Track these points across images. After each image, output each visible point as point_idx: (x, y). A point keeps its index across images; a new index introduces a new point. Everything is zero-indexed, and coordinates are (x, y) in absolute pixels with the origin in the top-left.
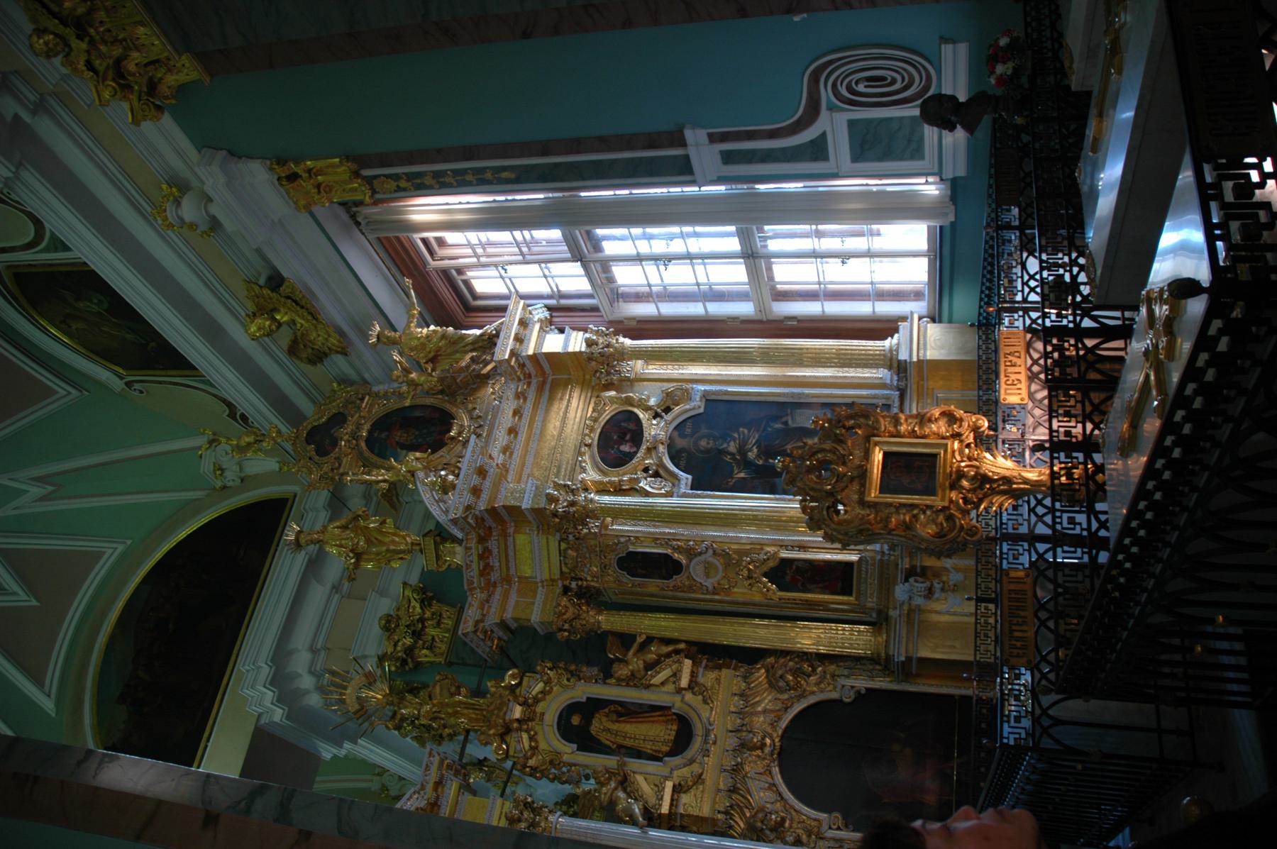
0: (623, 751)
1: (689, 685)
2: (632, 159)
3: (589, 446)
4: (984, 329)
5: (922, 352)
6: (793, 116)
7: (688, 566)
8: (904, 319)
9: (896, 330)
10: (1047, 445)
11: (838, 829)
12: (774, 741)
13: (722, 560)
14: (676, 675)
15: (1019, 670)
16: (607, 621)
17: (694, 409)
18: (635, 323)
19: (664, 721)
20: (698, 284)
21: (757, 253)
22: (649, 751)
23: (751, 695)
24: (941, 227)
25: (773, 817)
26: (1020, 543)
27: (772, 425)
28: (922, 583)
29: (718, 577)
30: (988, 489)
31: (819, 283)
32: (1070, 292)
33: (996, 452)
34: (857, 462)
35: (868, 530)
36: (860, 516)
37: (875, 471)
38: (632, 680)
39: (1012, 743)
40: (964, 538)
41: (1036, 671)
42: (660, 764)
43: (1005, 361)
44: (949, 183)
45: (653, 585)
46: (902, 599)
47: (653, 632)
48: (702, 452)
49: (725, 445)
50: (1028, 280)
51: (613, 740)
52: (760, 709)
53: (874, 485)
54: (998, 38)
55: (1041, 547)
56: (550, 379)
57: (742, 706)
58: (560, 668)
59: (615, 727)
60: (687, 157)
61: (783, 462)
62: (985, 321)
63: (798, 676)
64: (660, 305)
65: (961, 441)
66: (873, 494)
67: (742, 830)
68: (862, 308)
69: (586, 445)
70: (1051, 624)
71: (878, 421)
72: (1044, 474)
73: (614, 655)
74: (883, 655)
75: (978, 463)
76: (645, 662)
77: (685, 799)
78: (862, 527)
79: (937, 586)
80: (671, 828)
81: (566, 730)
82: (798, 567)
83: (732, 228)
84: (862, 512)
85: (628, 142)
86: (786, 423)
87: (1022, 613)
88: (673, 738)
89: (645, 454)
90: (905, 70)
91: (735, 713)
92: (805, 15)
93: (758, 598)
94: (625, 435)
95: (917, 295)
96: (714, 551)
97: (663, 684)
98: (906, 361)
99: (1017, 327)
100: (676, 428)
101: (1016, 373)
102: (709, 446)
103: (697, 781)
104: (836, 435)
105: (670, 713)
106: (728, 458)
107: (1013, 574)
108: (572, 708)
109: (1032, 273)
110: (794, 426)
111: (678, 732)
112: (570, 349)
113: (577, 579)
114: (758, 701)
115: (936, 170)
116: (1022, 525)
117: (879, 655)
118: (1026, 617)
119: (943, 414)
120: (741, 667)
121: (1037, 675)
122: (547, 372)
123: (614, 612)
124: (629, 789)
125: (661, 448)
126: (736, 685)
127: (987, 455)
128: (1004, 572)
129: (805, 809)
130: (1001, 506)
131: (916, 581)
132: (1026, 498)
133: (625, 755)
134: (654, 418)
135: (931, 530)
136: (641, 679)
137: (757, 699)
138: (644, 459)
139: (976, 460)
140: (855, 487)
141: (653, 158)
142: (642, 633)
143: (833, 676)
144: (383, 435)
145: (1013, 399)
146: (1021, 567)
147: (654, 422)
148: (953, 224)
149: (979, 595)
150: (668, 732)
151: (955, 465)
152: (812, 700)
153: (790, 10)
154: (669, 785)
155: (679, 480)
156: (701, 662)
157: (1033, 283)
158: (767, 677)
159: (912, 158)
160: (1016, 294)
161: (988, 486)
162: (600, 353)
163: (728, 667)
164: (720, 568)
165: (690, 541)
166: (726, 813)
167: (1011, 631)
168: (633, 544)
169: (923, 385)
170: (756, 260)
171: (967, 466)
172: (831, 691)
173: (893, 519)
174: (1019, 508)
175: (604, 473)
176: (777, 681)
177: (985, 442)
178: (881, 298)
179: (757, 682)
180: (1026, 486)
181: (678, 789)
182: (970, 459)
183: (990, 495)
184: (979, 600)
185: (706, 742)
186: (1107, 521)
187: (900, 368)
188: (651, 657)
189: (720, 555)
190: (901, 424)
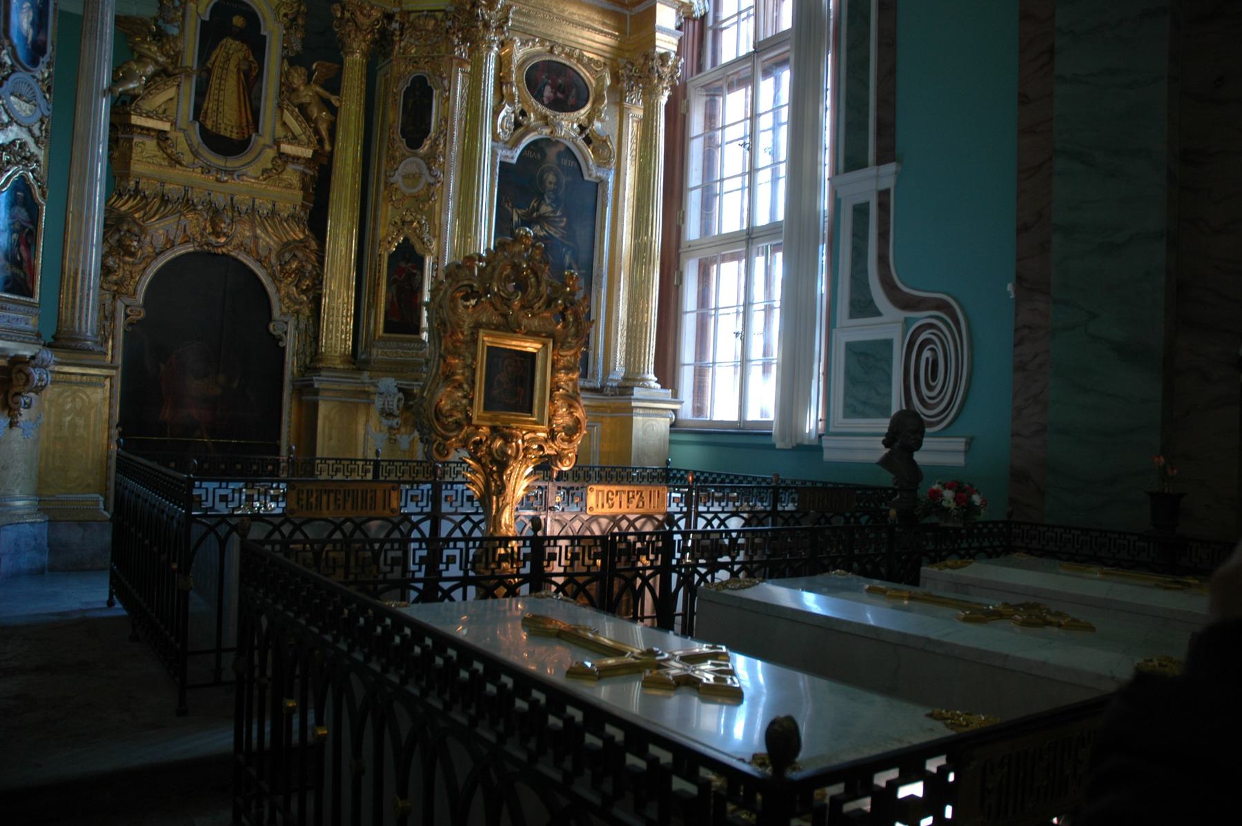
0: (204, 75)
1: (283, 154)
2: (867, 105)
3: (551, 51)
4: (664, 474)
5: (641, 411)
6: (903, 283)
7: (416, 155)
8: (675, 395)
9: (663, 387)
10: (540, 533)
11: (127, 316)
12: (223, 246)
13: (422, 192)
14: (294, 140)
15: (283, 501)
16: (355, 59)
17: (588, 169)
18: (682, 112)
19: (241, 123)
20: (722, 180)
21: (752, 244)
22: (205, 105)
23: (274, 223)
24: (770, 434)
25: (135, 243)
26: (430, 503)
27: (569, 252)
28: (398, 407)
29: (404, 189)
30: (491, 469)
31: (716, 309)
32: (711, 561)
33: (534, 478)
34: (525, 322)
35: (445, 332)
36: (461, 323)
37: (514, 343)
38: (286, 89)
39: (196, 492)
40: (435, 441)
41: (282, 519)
42: (191, 118)
43: (633, 492)
44: (816, 443)
45: (395, 117)
46: (380, 384)
47: (342, 113)
48: (541, 177)
50: (719, 519)
51: (216, 64)
52: (259, 231)
53: (498, 341)
54: (979, 494)
55: (426, 527)
56: (627, 12)
57: (261, 212)
58: (299, 6)
59: (232, 66)
60: (864, 165)
61: (526, 236)
62: (671, 475)
63: (296, 274)
64: (701, 140)
65: (546, 440)
66: (487, 339)
67: (118, 209)
68: (687, 353)
69: (552, 48)
70: (338, 535)
71: (571, 348)
72: (508, 530)
73: (315, 70)
74: (321, 365)
75: (521, 458)
76: (309, 104)
77: (151, 144)
78: (449, 325)
79: (394, 422)
80: (113, 126)
82: (415, 274)
83: (780, 216)
84: (466, 327)
85: (887, 101)
87: (349, 505)
88: (222, 133)
89: (541, 113)
90: (942, 400)
91: (253, 205)
92: (1012, 296)
93: (382, 232)
94: (563, 92)
95: (698, 410)
96: (433, 185)
97: (284, 124)
98: (632, 394)
99: (670, 506)
100: (568, 149)
101: (621, 502)
102: (548, 185)
103: (172, 159)
104: (557, 299)
105: (251, 131)
106: (534, 204)
107: (394, 495)
111: (230, 140)
112: (658, 35)
113: (402, 29)
114: (267, 231)
115: (832, 430)
116: (451, 506)
117: (321, 360)
118: (344, 508)
119: (578, 421)
120: (306, 213)
121: (277, 521)
122: (633, 9)
123: (364, 72)
124: (158, 79)
125: (546, 131)
126: (285, 206)
127: (530, 469)
128: (396, 485)
129: (146, 280)
130: (473, 483)
131: (399, 400)
132: (481, 511)
133: (199, 76)
134: (580, 126)
135: (445, 405)
136: (289, 99)
137: (269, 229)
138: (535, 112)
139: (525, 456)
140: (496, 319)
141: (866, 129)
142: (341, 102)
143: (297, 312)
145: (592, 499)
146: (403, 504)
147: (575, 126)
148: (772, 447)
149: (382, 463)
150: (229, 129)
151: (518, 433)
152: (271, 289)
153: (1019, 280)
154: (166, 126)
155: (511, 149)
156: (309, 168)
157: (716, 523)
158: (295, 240)
159: (846, 406)
160: (705, 505)
161: (494, 469)
162: (653, 68)
163: (304, 198)
164: (414, 191)
165: (444, 158)
166: (137, 191)
167: (328, 492)
168: (441, 94)
169: (606, 412)
170: (744, 242)
171: (518, 446)
172: (281, 309)
173: (457, 361)
174: (470, 503)
175: (520, 66)
176: (290, 251)
177: (544, 467)
178: (697, 373)
179: (288, 229)
180: (494, 511)
181: (161, 136)
182: (526, 449)
183: (484, 471)
184: (377, 464)
185: (219, 170)
186: (452, 599)
187: (625, 389)
188: (314, 112)
189: (428, 190)
190: (567, 374)
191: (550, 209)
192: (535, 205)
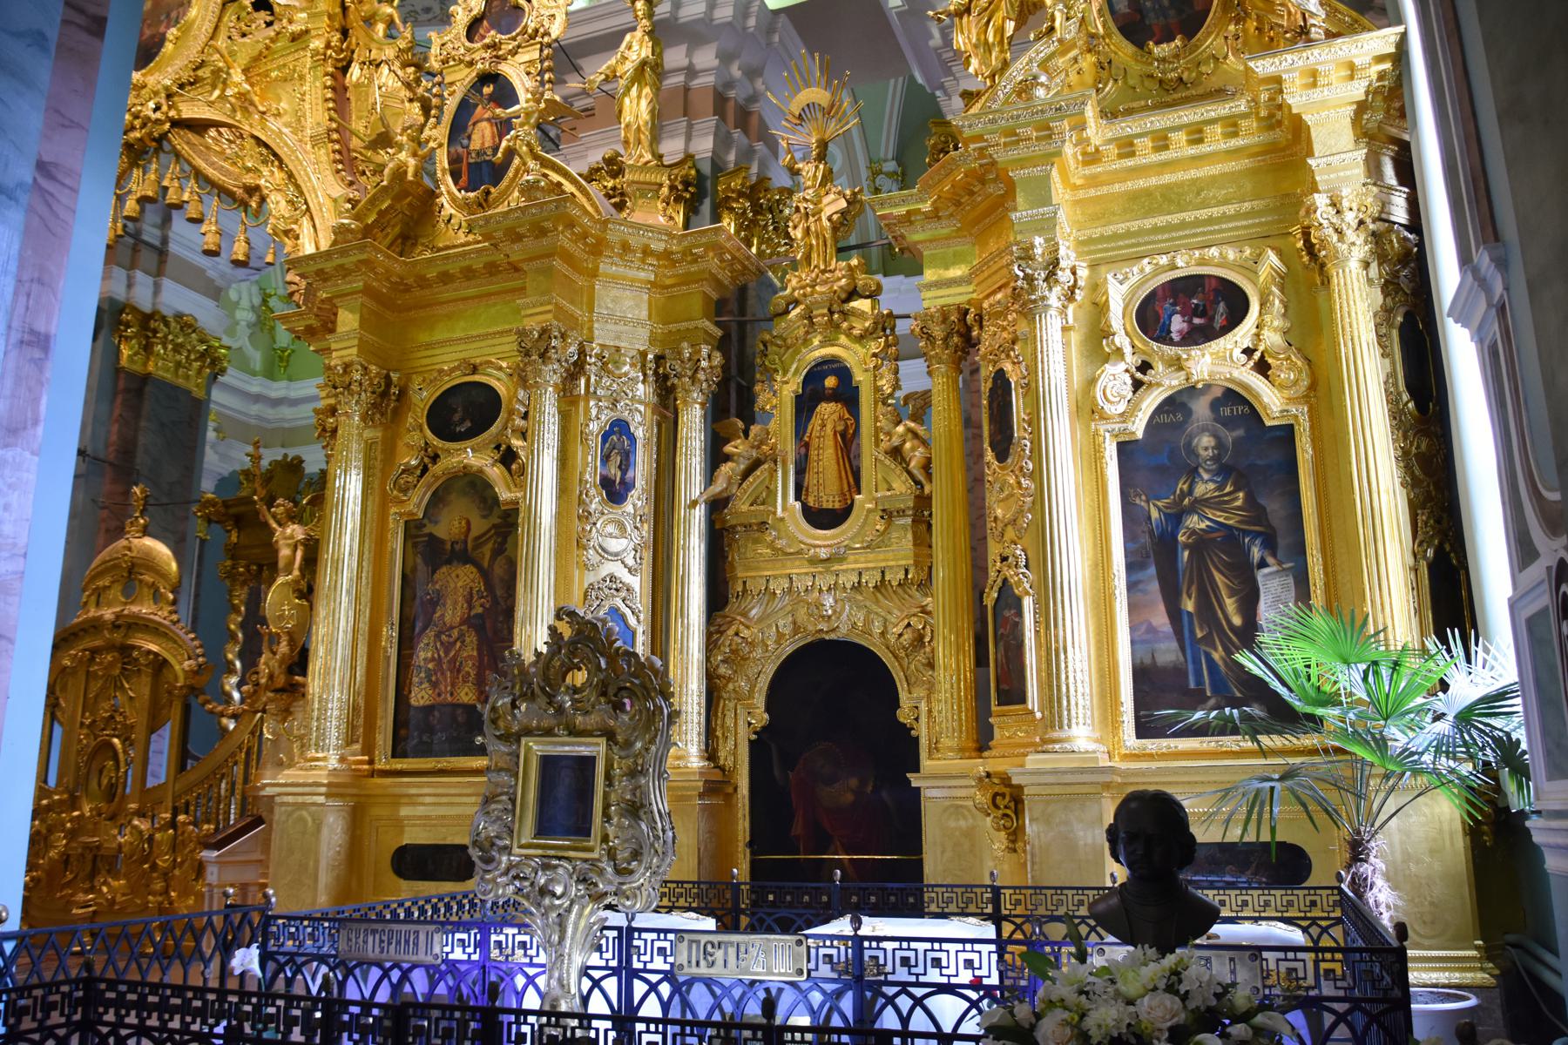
0: (803, 450)
19: (842, 489)
27: (1258, 542)
48: (1188, 445)
49: (1206, 476)
50: (911, 996)
86: (1263, 564)
87: (393, 947)
88: (825, 506)
102: (1202, 452)
106: (1183, 486)
108: (844, 373)
109: (926, 1002)
110: (1260, 579)
111: (832, 511)
142: (929, 430)
150: (831, 499)
191: (1211, 486)
192: (1185, 487)
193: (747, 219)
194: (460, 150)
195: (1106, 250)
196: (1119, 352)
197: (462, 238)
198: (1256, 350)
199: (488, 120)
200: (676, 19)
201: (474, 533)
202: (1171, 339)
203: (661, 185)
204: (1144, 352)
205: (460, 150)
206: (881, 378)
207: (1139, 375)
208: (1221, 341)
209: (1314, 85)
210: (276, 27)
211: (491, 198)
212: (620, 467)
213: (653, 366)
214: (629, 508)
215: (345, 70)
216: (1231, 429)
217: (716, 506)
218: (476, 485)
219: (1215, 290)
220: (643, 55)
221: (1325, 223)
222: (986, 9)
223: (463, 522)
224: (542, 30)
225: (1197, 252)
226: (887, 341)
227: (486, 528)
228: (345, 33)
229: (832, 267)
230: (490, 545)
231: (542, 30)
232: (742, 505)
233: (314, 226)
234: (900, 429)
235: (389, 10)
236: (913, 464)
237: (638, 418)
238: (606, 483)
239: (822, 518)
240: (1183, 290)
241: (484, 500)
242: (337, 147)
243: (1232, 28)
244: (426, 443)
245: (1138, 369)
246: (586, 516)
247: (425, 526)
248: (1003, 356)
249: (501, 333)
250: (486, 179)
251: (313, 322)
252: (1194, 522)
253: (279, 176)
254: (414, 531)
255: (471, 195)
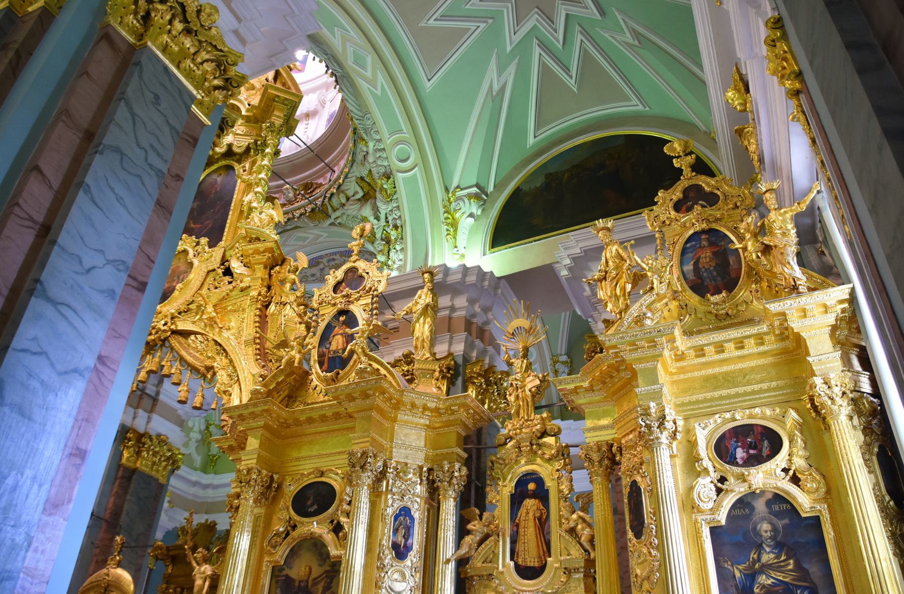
0: (515, 529)
19: (539, 554)
48: (755, 529)
49: (768, 550)
81: (522, 482)
88: (529, 564)
102: (764, 534)
106: (753, 556)
108: (540, 481)
111: (534, 568)
142: (592, 517)
144: (705, 243)
150: (533, 560)
192: (755, 556)
193: (482, 388)
194: (325, 350)
195: (693, 410)
196: (706, 470)
197: (321, 398)
198: (790, 469)
199: (341, 334)
200: (446, 282)
201: (314, 575)
202: (737, 463)
203: (435, 371)
204: (721, 471)
205: (325, 350)
206: (562, 485)
207: (719, 485)
208: (768, 464)
209: (805, 316)
210: (234, 284)
211: (339, 376)
212: (404, 537)
213: (426, 474)
214: (408, 562)
215: (267, 307)
216: (781, 519)
217: (462, 563)
218: (317, 545)
219: (761, 433)
220: (427, 301)
221: (822, 394)
222: (615, 278)
223: (308, 568)
224: (373, 288)
225: (747, 411)
226: (565, 462)
227: (320, 573)
228: (269, 288)
229: (532, 418)
230: (322, 584)
231: (373, 288)
232: (477, 563)
233: (241, 389)
234: (574, 516)
235: (293, 277)
236: (583, 539)
237: (416, 506)
238: (395, 546)
239: (528, 573)
240: (741, 433)
241: (321, 554)
242: (258, 347)
243: (753, 286)
244: (290, 518)
245: (719, 481)
246: (382, 568)
247: (284, 569)
248: (635, 472)
249: (339, 453)
250: (338, 366)
251: (233, 443)
252: (763, 579)
253: (225, 361)
254: (277, 573)
255: (329, 374)
